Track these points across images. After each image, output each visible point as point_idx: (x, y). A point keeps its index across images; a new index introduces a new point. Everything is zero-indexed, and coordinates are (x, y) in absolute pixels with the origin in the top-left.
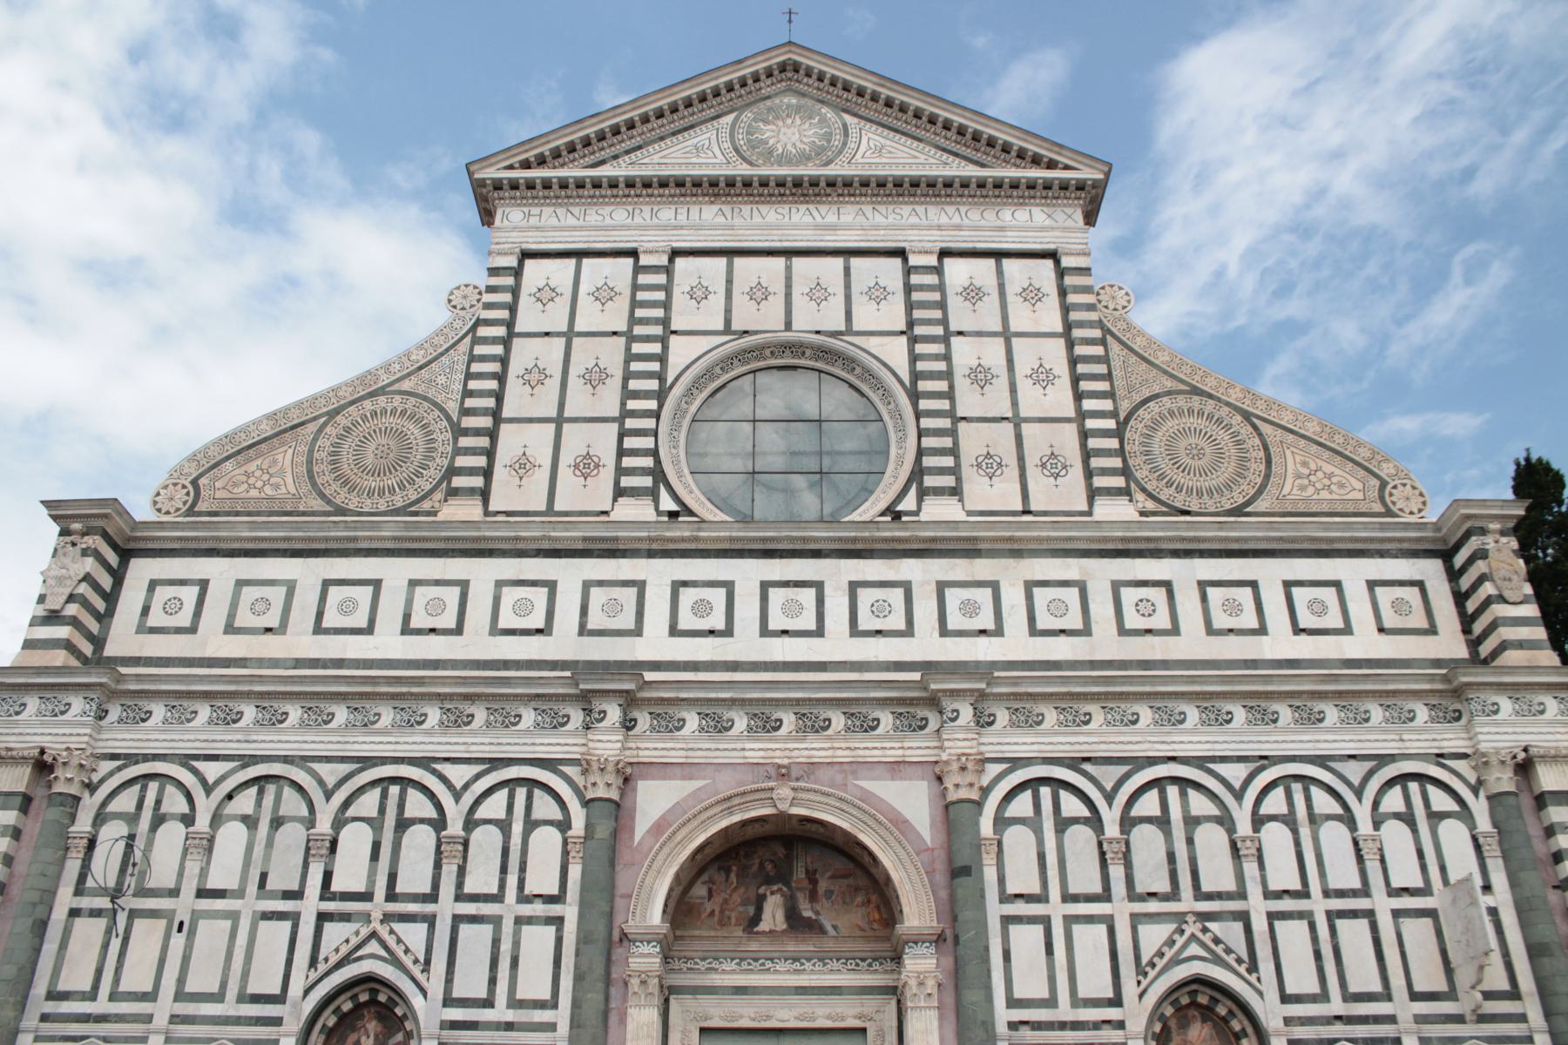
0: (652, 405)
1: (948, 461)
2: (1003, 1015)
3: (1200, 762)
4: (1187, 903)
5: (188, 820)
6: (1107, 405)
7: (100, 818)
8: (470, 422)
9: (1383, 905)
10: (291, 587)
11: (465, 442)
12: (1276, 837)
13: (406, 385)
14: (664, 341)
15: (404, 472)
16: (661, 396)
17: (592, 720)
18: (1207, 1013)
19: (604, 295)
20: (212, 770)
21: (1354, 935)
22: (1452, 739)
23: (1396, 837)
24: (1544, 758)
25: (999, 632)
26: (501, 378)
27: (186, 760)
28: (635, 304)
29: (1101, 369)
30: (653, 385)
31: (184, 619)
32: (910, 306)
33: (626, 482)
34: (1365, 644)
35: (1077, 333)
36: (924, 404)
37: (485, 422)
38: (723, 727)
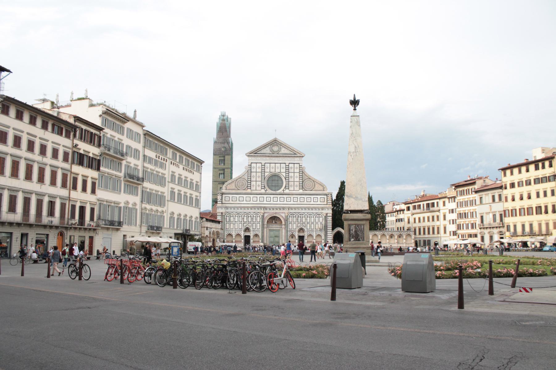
0: (264, 180)
1: (288, 186)
2: (289, 230)
3: (304, 213)
4: (301, 223)
5: (233, 217)
6: (302, 180)
7: (227, 217)
8: (249, 182)
9: (315, 223)
10: (236, 197)
11: (248, 184)
12: (308, 218)
13: (243, 177)
14: (264, 173)
15: (244, 186)
16: (264, 179)
17: (261, 209)
18: (302, 230)
19: (259, 168)
20: (234, 213)
21: (312, 225)
22: (322, 211)
23: (317, 218)
24: (329, 213)
25: (291, 201)
26: (251, 177)
27: (232, 212)
28: (262, 169)
29: (302, 177)
30: (264, 178)
31: (228, 200)
32: (286, 170)
33: (262, 188)
34: (319, 203)
35: (300, 173)
36: (286, 180)
37: (250, 182)
38: (270, 209)
